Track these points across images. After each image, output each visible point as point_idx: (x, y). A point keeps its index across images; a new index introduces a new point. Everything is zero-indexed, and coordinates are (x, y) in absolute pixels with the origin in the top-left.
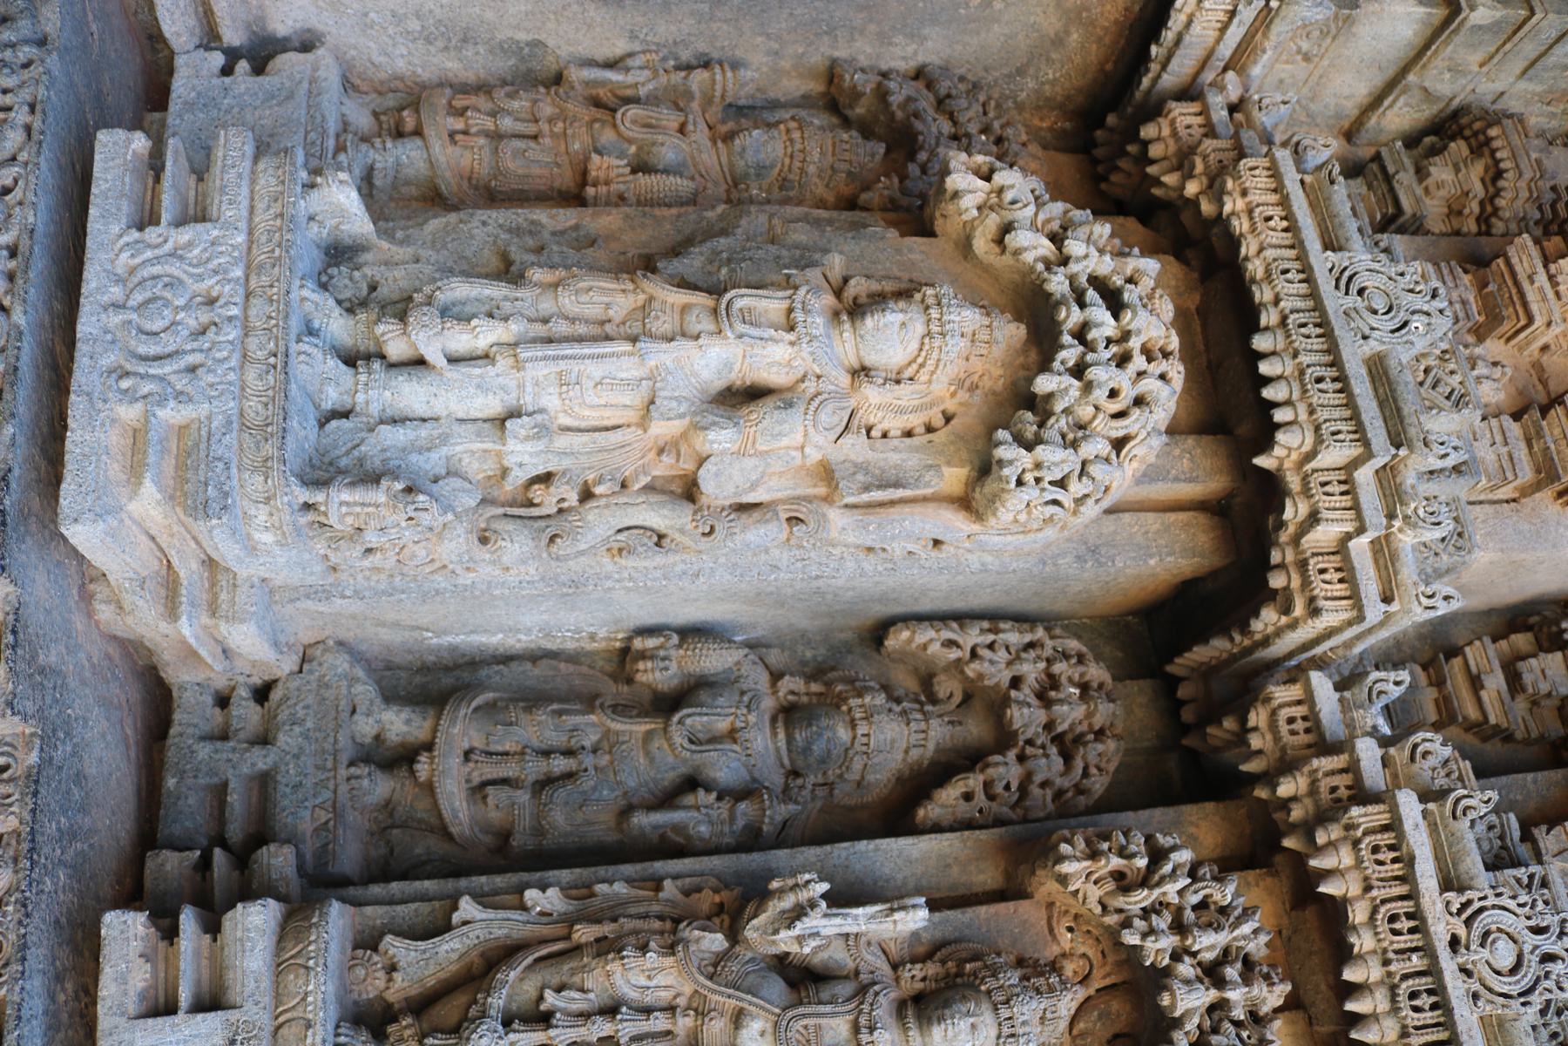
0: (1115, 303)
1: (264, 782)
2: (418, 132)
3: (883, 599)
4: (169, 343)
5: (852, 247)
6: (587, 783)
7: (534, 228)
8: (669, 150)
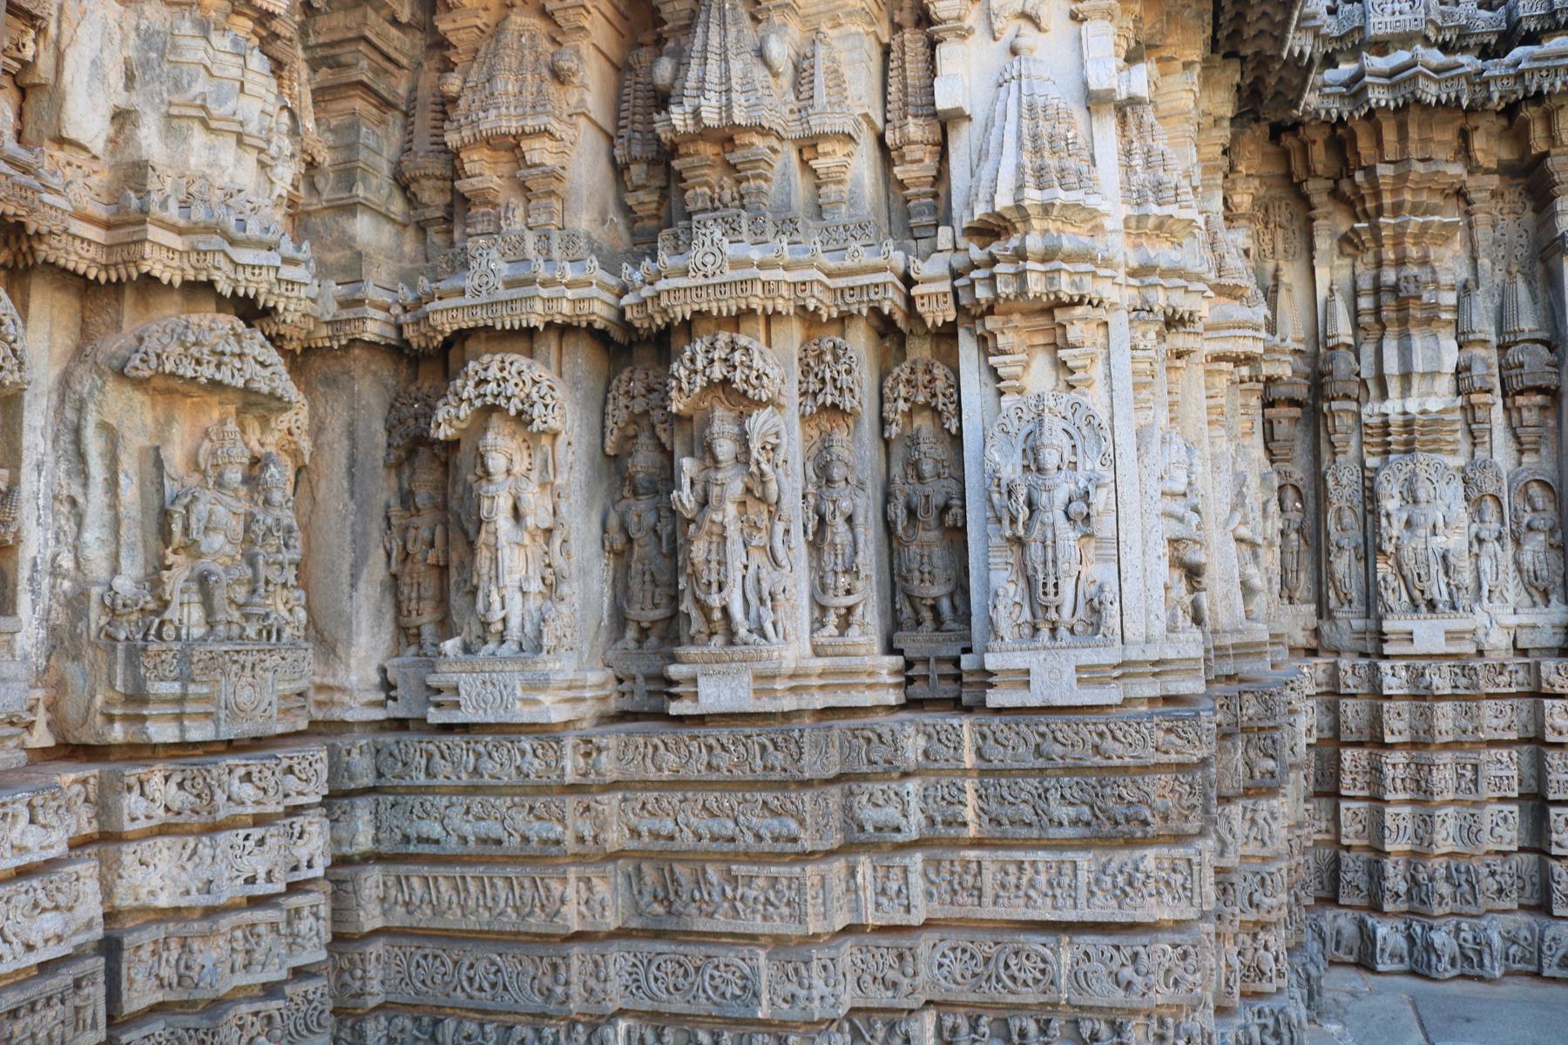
0: (485, 381)
1: (648, 678)
2: (418, 628)
3: (592, 459)
4: (497, 694)
5: (464, 471)
6: (653, 568)
7: (457, 583)
8: (425, 534)
